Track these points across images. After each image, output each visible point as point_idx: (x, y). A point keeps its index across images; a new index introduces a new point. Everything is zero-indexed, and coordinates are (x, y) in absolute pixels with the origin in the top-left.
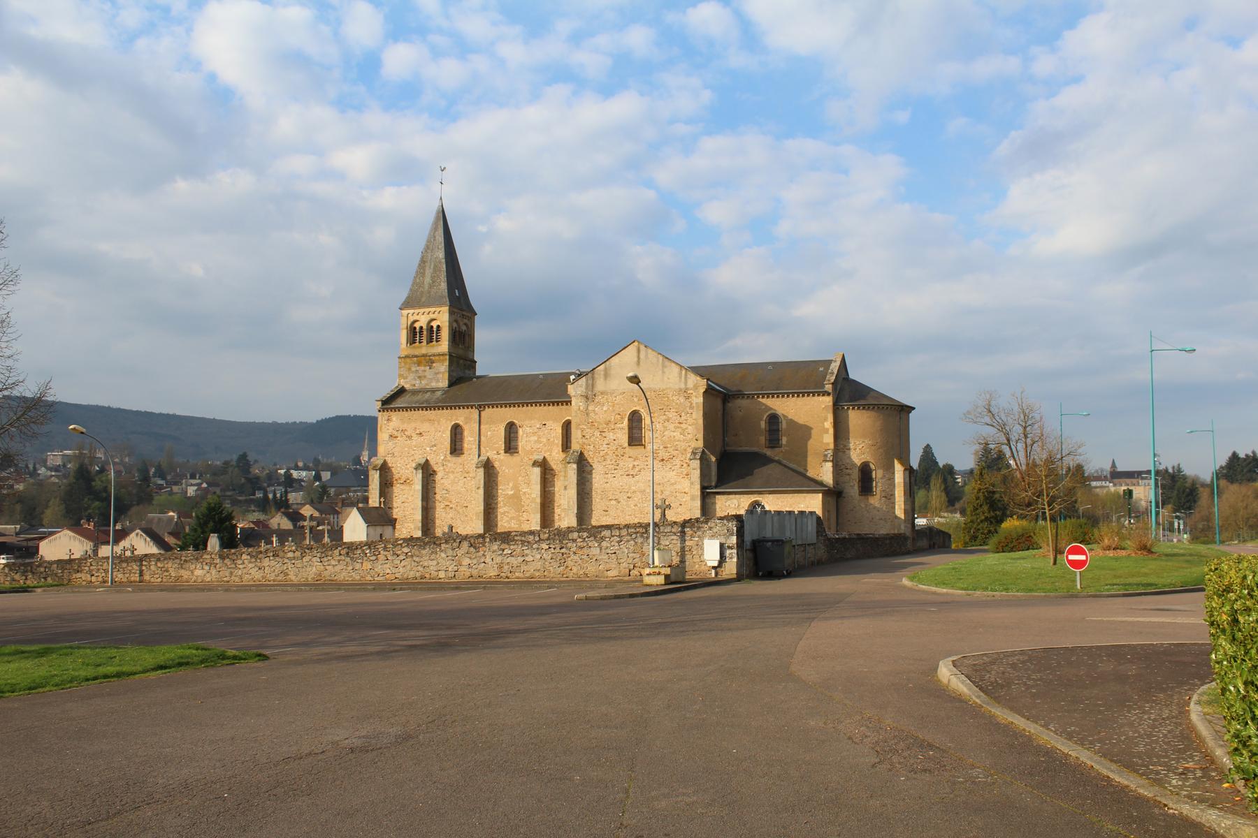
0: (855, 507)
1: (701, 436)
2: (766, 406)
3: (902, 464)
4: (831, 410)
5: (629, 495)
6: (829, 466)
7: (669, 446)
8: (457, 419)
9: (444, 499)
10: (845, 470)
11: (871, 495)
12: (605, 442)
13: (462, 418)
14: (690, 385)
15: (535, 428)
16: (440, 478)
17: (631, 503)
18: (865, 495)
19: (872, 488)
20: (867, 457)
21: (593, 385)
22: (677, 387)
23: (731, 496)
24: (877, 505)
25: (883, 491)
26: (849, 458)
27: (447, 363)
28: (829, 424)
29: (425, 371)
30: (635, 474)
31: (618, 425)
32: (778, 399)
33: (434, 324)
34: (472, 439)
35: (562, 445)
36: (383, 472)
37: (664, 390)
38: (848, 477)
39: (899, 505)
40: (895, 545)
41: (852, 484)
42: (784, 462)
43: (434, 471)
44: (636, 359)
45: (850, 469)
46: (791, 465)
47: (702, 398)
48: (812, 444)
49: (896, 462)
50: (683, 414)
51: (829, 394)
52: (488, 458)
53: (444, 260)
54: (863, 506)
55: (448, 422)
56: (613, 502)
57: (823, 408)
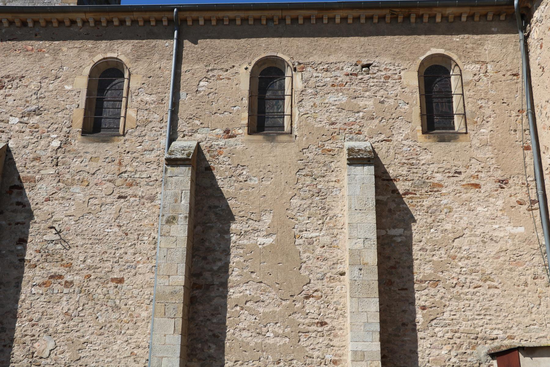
8: (112, 51)
9: (48, 256)
15: (337, 73)
16: (40, 198)
34: (154, 97)
35: (422, 115)
52: (198, 146)
55: (85, 55)
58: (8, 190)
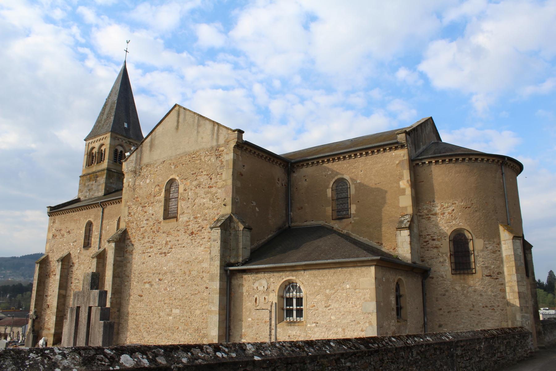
0: (447, 291)
1: (229, 200)
2: (333, 171)
3: (510, 231)
4: (407, 166)
5: (161, 277)
6: (405, 235)
7: (199, 215)
8: (90, 218)
10: (431, 242)
11: (468, 274)
12: (146, 218)
13: (93, 216)
14: (222, 141)
17: (162, 286)
18: (460, 274)
19: (469, 263)
20: (460, 223)
21: (141, 158)
22: (209, 146)
23: (260, 275)
24: (478, 287)
25: (487, 267)
26: (436, 225)
27: (105, 177)
28: (405, 184)
29: (92, 185)
30: (166, 251)
31: (157, 198)
32: (345, 161)
33: (103, 148)
36: (65, 267)
37: (198, 151)
38: (435, 250)
39: (511, 287)
40: (502, 348)
41: (442, 260)
42: (354, 235)
43: (73, 263)
44: (176, 124)
45: (438, 240)
46: (362, 239)
47: (232, 154)
48: (388, 211)
49: (501, 228)
50: (213, 176)
51: (402, 146)
53: (116, 102)
54: (458, 288)
56: (147, 286)
57: (397, 164)
58: (69, 267)
